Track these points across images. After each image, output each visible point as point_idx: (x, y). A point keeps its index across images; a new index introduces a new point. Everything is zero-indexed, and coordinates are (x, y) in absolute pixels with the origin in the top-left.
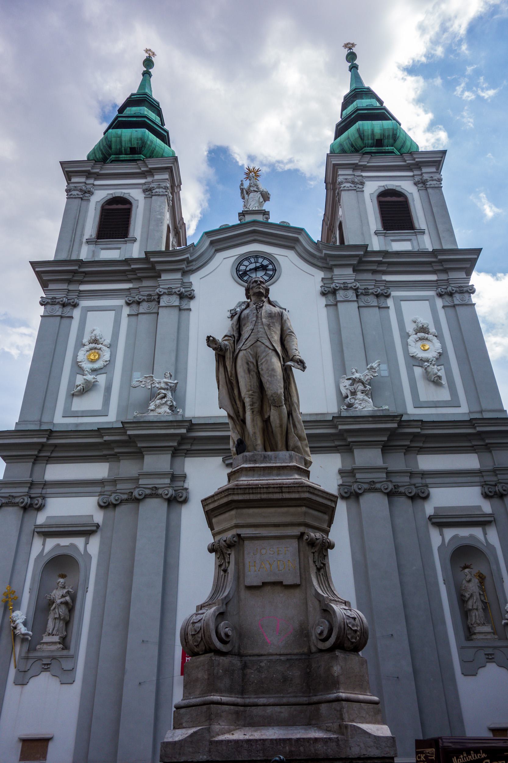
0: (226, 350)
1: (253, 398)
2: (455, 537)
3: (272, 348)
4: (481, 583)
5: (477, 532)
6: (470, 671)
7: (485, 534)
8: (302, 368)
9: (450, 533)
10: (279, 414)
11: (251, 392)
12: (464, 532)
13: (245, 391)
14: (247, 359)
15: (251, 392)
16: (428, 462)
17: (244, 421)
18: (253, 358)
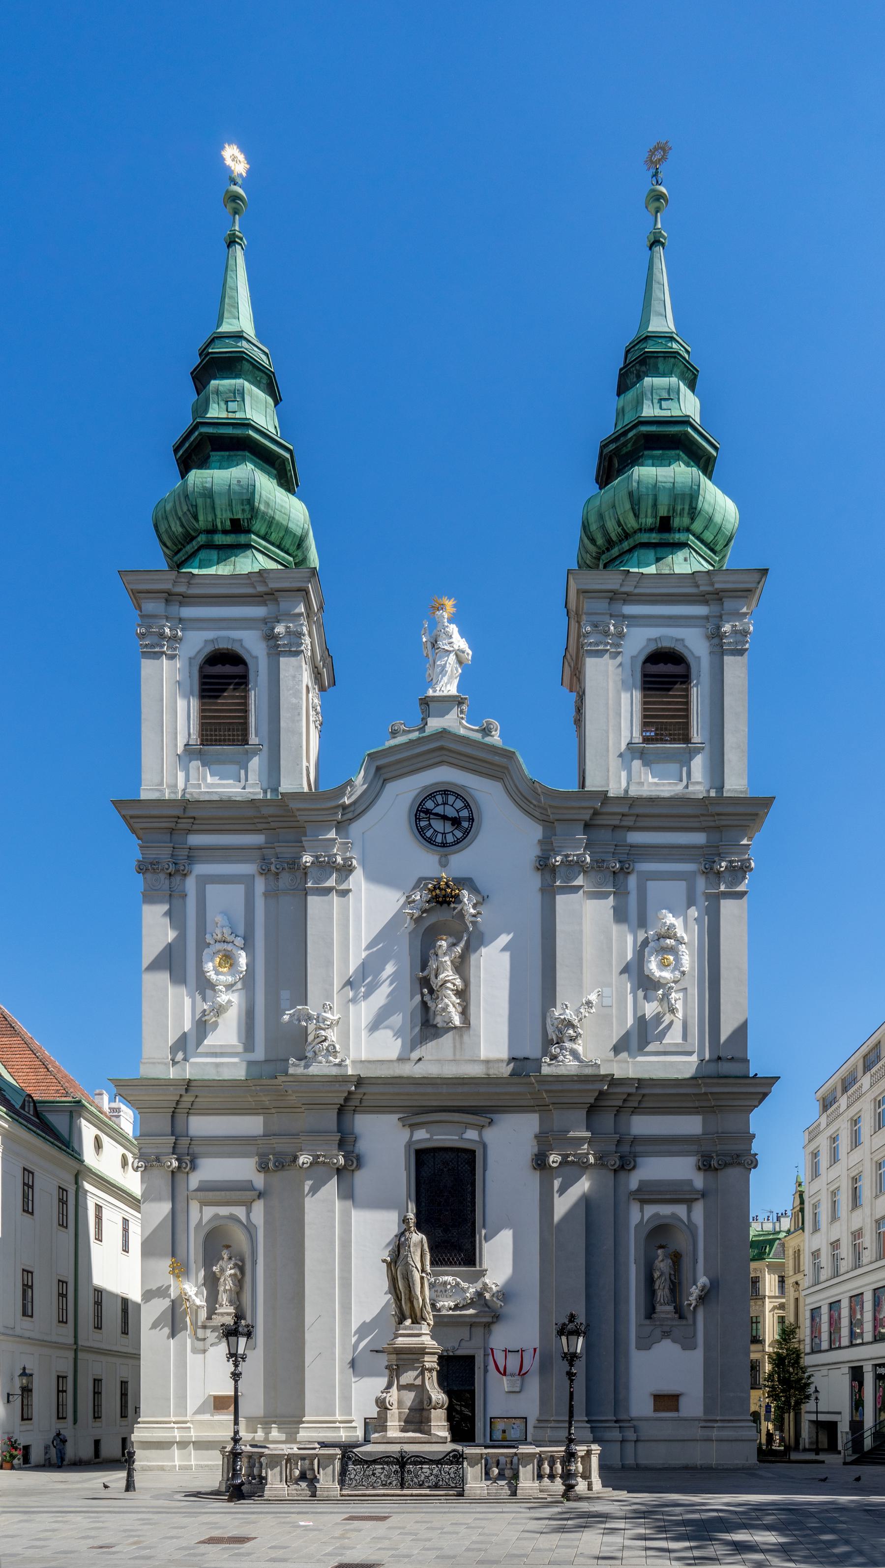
2: (656, 1216)
4: (674, 1263)
5: (680, 1210)
6: (645, 1344)
7: (689, 1211)
9: (650, 1210)
12: (666, 1210)
16: (643, 1125)
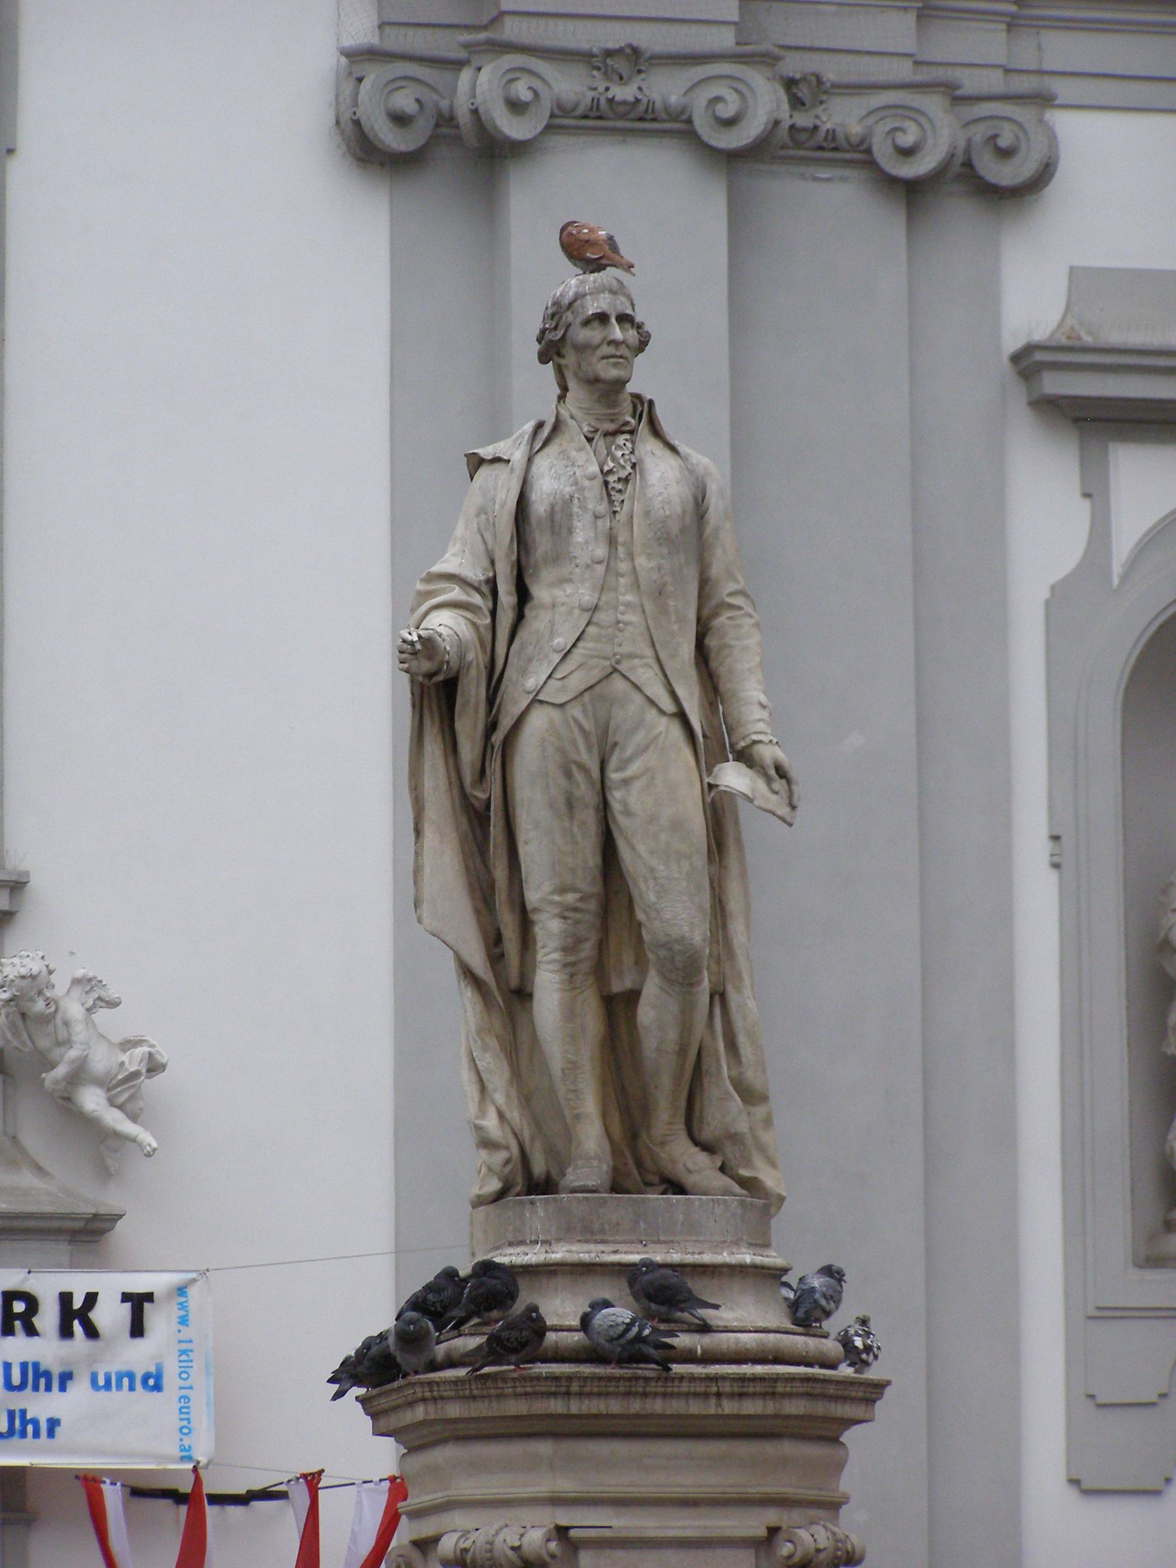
0: (463, 666)
1: (577, 922)
3: (668, 705)
8: (784, 810)
10: (683, 1012)
11: (571, 898)
13: (547, 887)
14: (562, 751)
15: (571, 898)
17: (522, 995)
18: (589, 748)
